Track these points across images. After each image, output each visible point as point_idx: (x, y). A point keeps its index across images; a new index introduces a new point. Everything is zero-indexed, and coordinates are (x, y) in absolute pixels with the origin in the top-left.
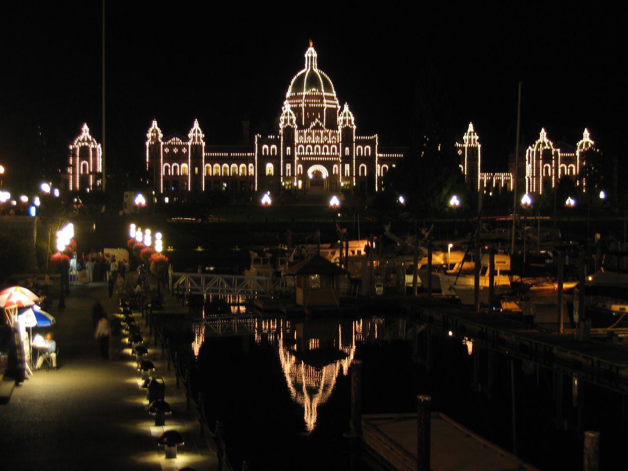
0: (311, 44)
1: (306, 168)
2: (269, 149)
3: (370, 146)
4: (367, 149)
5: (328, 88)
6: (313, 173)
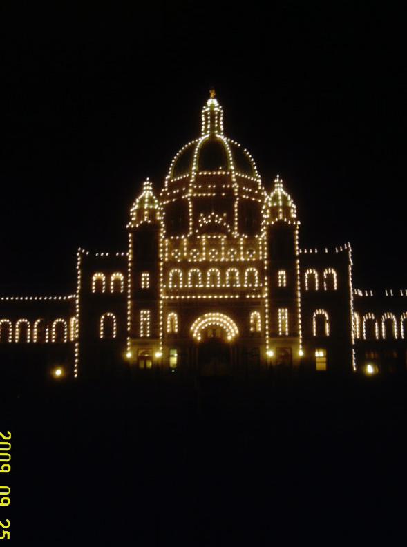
0: (213, 94)
1: (186, 321)
2: (108, 280)
3: (336, 270)
4: (330, 276)
5: (243, 165)
6: (204, 332)
